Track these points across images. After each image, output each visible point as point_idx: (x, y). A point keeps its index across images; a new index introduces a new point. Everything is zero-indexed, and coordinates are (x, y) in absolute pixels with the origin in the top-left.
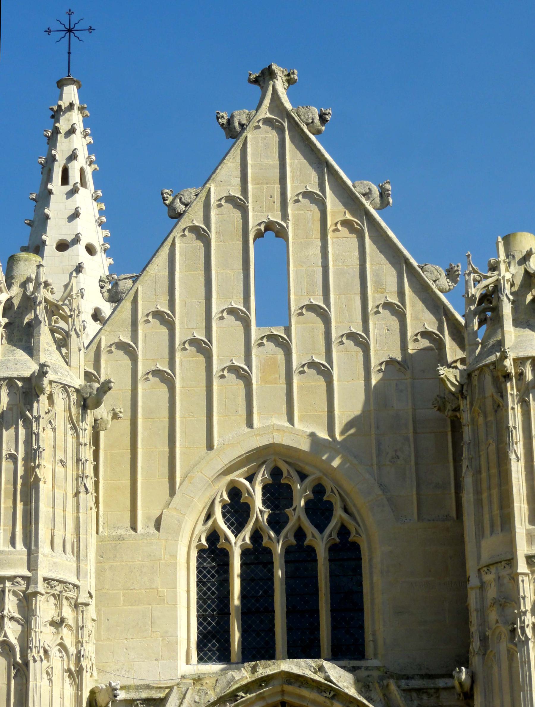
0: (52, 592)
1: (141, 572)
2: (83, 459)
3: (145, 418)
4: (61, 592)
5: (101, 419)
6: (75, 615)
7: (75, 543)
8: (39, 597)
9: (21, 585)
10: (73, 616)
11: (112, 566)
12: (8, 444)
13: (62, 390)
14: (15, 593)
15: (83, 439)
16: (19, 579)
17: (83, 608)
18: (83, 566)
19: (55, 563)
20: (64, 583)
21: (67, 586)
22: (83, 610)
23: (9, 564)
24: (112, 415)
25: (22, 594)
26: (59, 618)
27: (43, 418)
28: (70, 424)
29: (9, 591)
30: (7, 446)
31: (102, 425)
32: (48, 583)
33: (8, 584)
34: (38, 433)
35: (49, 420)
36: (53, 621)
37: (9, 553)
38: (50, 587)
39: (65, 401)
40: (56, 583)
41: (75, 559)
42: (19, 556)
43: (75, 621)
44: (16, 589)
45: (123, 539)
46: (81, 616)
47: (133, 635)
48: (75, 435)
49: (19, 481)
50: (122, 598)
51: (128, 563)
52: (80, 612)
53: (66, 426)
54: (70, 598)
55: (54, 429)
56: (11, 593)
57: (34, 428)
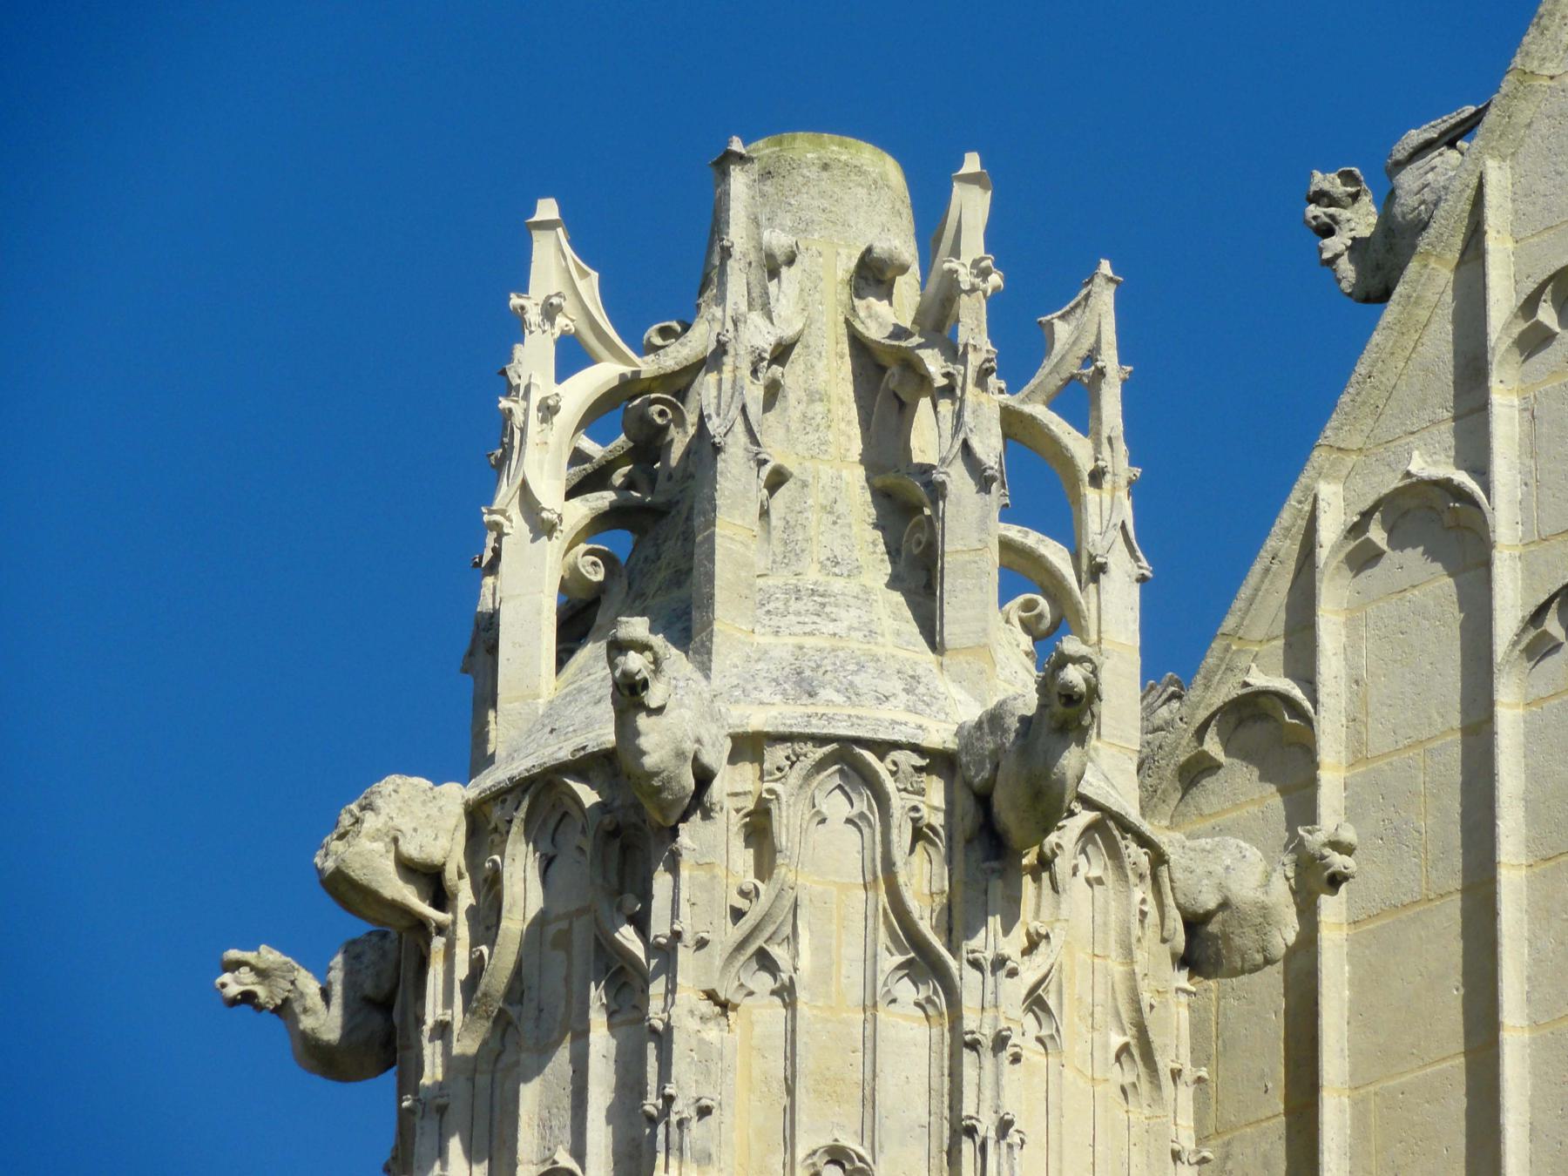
2: (987, 1127)
5: (1225, 905)
12: (545, 1126)
13: (841, 771)
15: (990, 1013)
24: (1291, 874)
27: (702, 944)
28: (902, 951)
30: (543, 1138)
31: (1237, 941)
34: (669, 1028)
35: (752, 949)
39: (866, 830)
48: (941, 1001)
53: (870, 960)
55: (786, 994)
57: (655, 1006)
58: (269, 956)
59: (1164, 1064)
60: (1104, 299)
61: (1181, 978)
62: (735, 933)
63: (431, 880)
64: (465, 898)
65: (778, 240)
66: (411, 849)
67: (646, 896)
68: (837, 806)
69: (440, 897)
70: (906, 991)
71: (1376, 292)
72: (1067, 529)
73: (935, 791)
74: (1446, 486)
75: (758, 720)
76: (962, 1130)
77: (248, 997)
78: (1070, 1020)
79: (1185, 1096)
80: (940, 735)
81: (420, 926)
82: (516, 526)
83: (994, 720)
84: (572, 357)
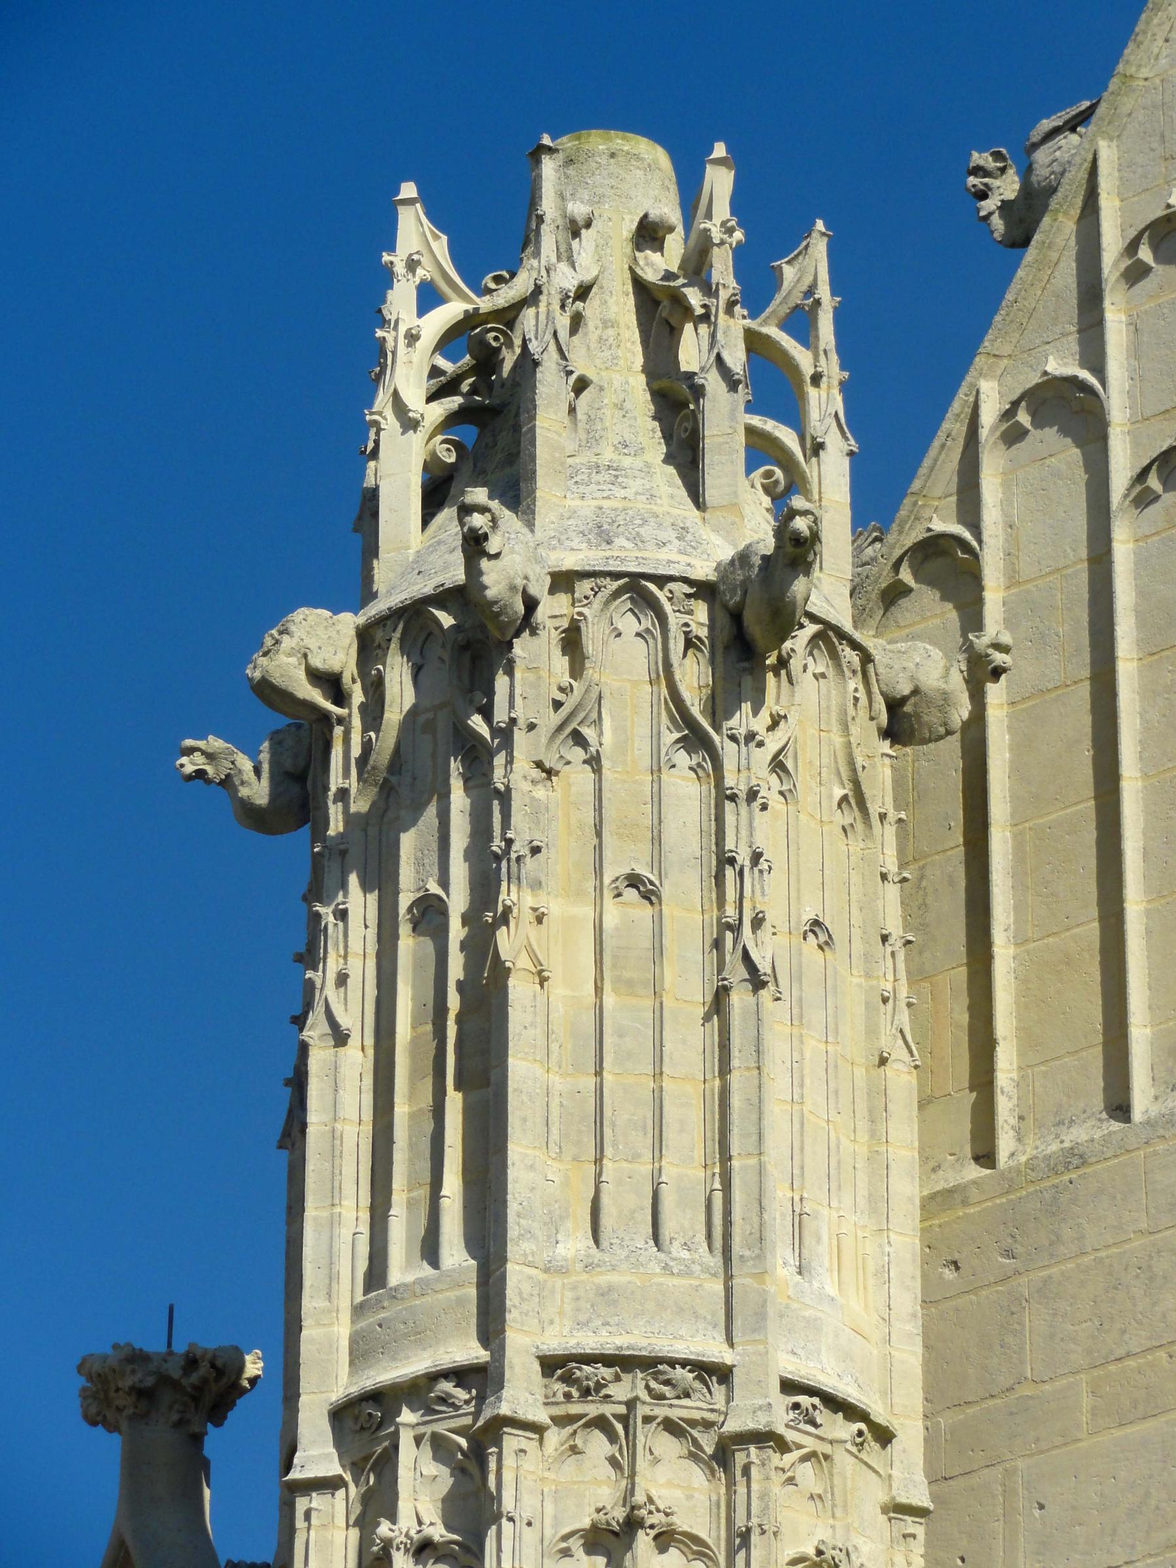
0: (592, 1409)
1: (1152, 1279)
2: (743, 858)
3: (1150, 651)
4: (631, 1404)
5: (916, 692)
6: (723, 1490)
7: (718, 1197)
8: (512, 1441)
9: (457, 1408)
10: (714, 1498)
11: (1047, 1280)
12: (419, 863)
13: (631, 598)
14: (440, 1447)
15: (744, 774)
16: (446, 1386)
17: (748, 1456)
18: (748, 1281)
19: (605, 1293)
20: (648, 1364)
21: (661, 1377)
22: (750, 1463)
23: (419, 1336)
24: (964, 668)
25: (463, 1442)
26: (620, 1514)
27: (532, 727)
28: (679, 729)
29: (418, 1440)
30: (418, 872)
31: (926, 718)
32: (567, 1379)
33: (407, 1416)
34: (508, 789)
35: (568, 730)
36: (595, 1527)
37: (418, 1291)
38: (575, 1393)
39: (651, 641)
40: (606, 1372)
41: (716, 1261)
42: (451, 1294)
43: (723, 1515)
44: (440, 1428)
45: (1084, 1162)
46: (741, 1489)
47: (1133, 1547)
48: (709, 766)
49: (454, 1001)
50: (1086, 1401)
51: (1103, 1254)
52: (738, 1473)
53: (656, 737)
54: (693, 1423)
55: (594, 762)
56: (427, 1449)
57: (498, 773)
58: (215, 743)
59: (874, 809)
60: (819, 248)
61: (885, 746)
62: (556, 718)
63: (331, 684)
64: (358, 696)
65: (578, 209)
66: (317, 662)
67: (490, 693)
68: (629, 624)
69: (339, 696)
70: (683, 758)
71: (1019, 239)
72: (794, 416)
73: (701, 612)
74: (1073, 381)
75: (570, 562)
76: (725, 860)
77: (200, 774)
78: (804, 777)
79: (890, 832)
80: (704, 570)
81: (325, 719)
82: (390, 423)
83: (743, 558)
84: (429, 298)
